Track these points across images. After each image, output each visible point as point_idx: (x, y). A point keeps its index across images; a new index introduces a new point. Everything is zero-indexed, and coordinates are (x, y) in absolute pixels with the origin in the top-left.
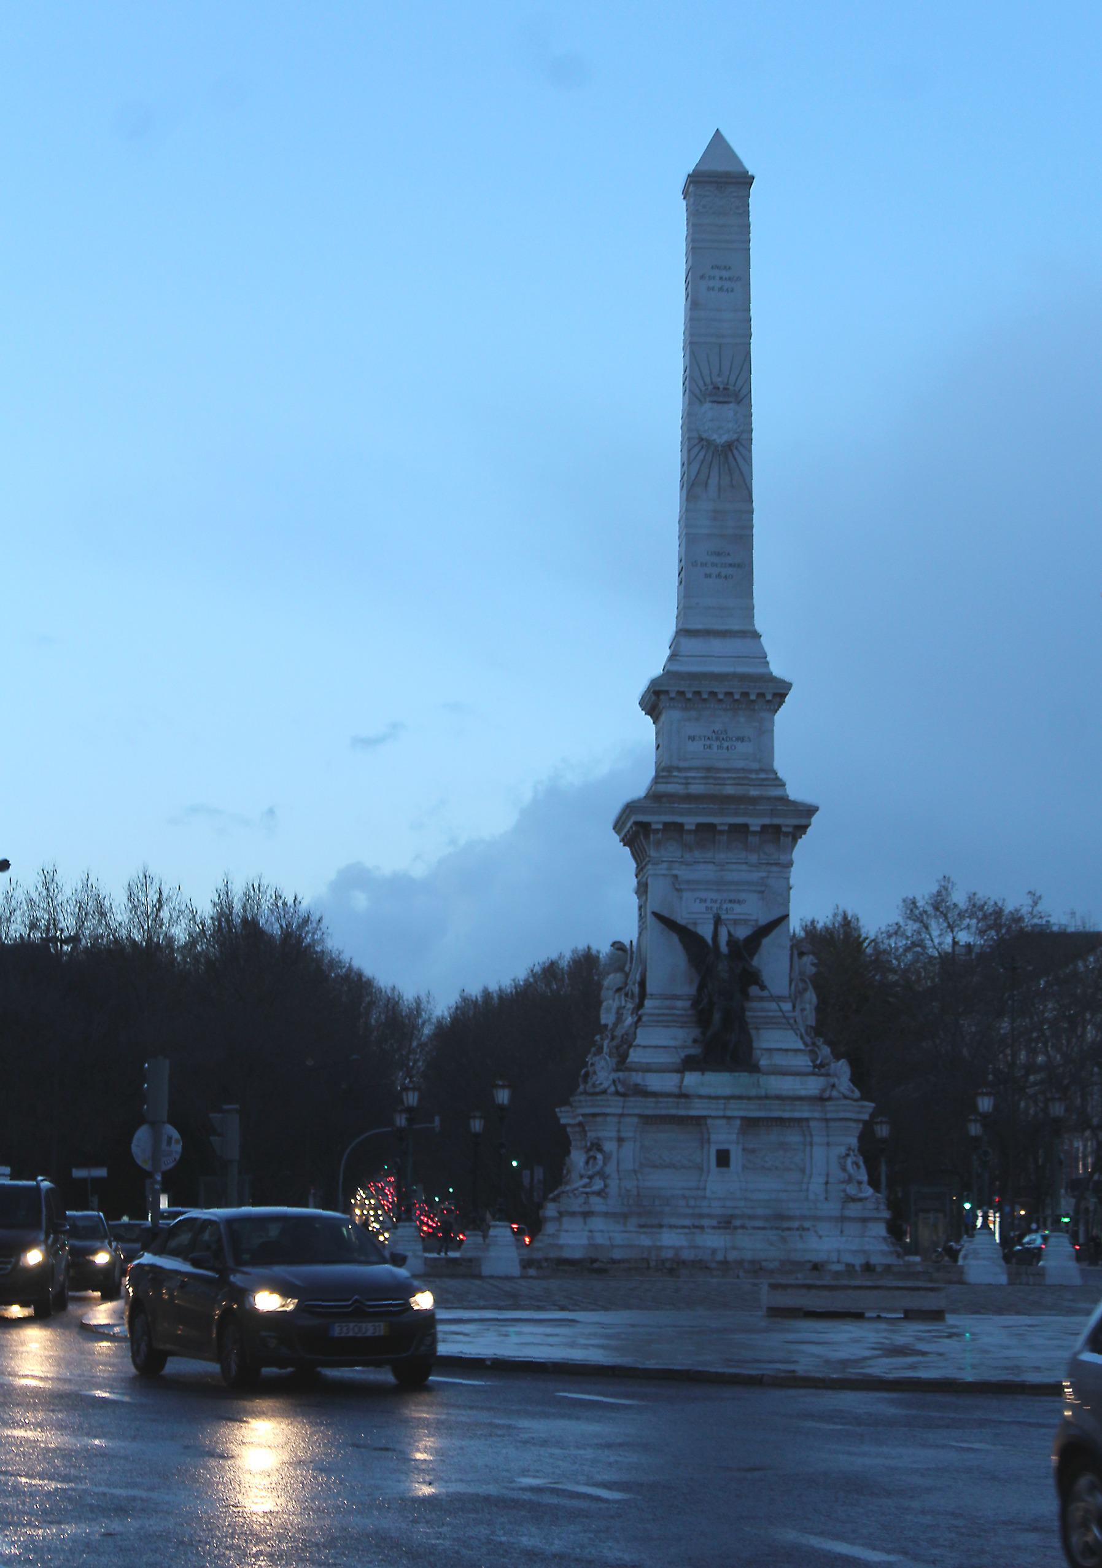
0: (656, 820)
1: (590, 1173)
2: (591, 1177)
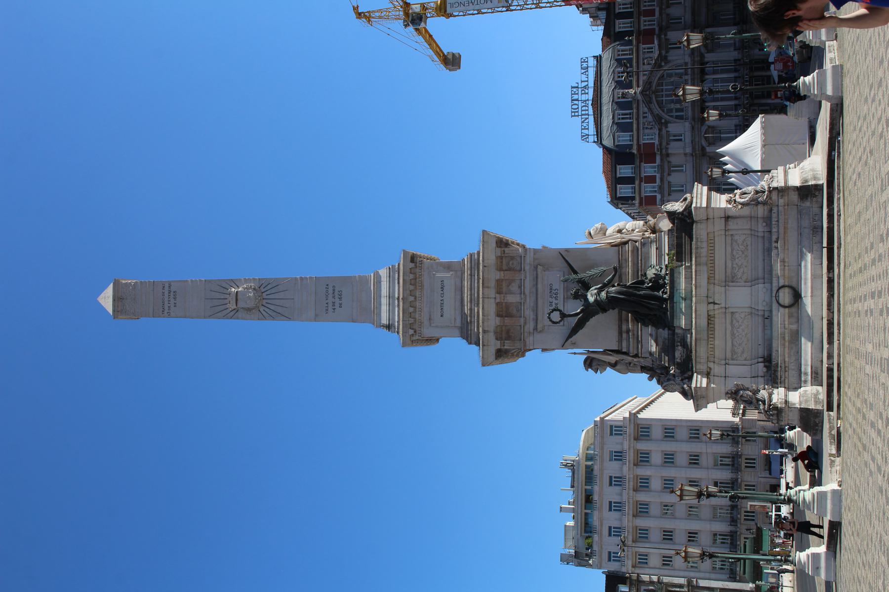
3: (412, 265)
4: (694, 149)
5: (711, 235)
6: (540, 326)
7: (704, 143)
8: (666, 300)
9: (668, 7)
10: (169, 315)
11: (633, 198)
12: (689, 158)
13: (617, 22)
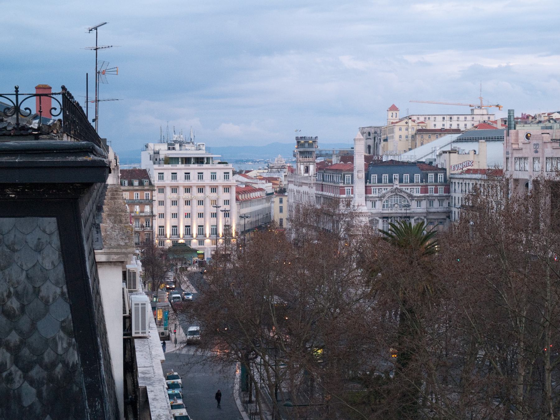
11: (344, 183)
13: (433, 174)
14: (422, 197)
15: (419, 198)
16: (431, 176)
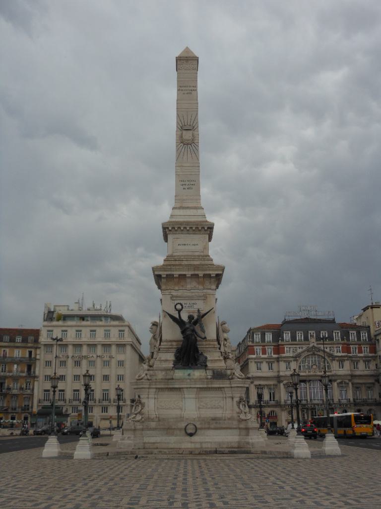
0: (164, 274)
1: (136, 412)
2: (136, 414)
3: (206, 229)
4: (282, 376)
5: (223, 389)
6: (174, 298)
7: (285, 382)
8: (188, 365)
9: (364, 361)
10: (178, 90)
11: (253, 342)
12: (276, 374)
14: (344, 357)
15: (340, 359)
16: (353, 335)
